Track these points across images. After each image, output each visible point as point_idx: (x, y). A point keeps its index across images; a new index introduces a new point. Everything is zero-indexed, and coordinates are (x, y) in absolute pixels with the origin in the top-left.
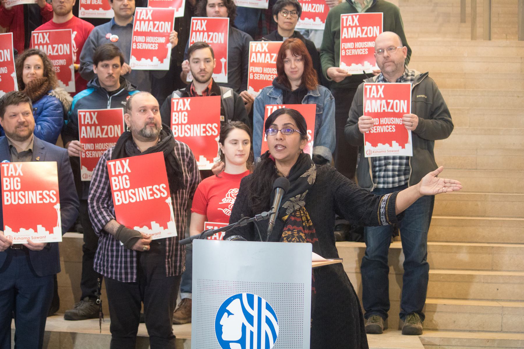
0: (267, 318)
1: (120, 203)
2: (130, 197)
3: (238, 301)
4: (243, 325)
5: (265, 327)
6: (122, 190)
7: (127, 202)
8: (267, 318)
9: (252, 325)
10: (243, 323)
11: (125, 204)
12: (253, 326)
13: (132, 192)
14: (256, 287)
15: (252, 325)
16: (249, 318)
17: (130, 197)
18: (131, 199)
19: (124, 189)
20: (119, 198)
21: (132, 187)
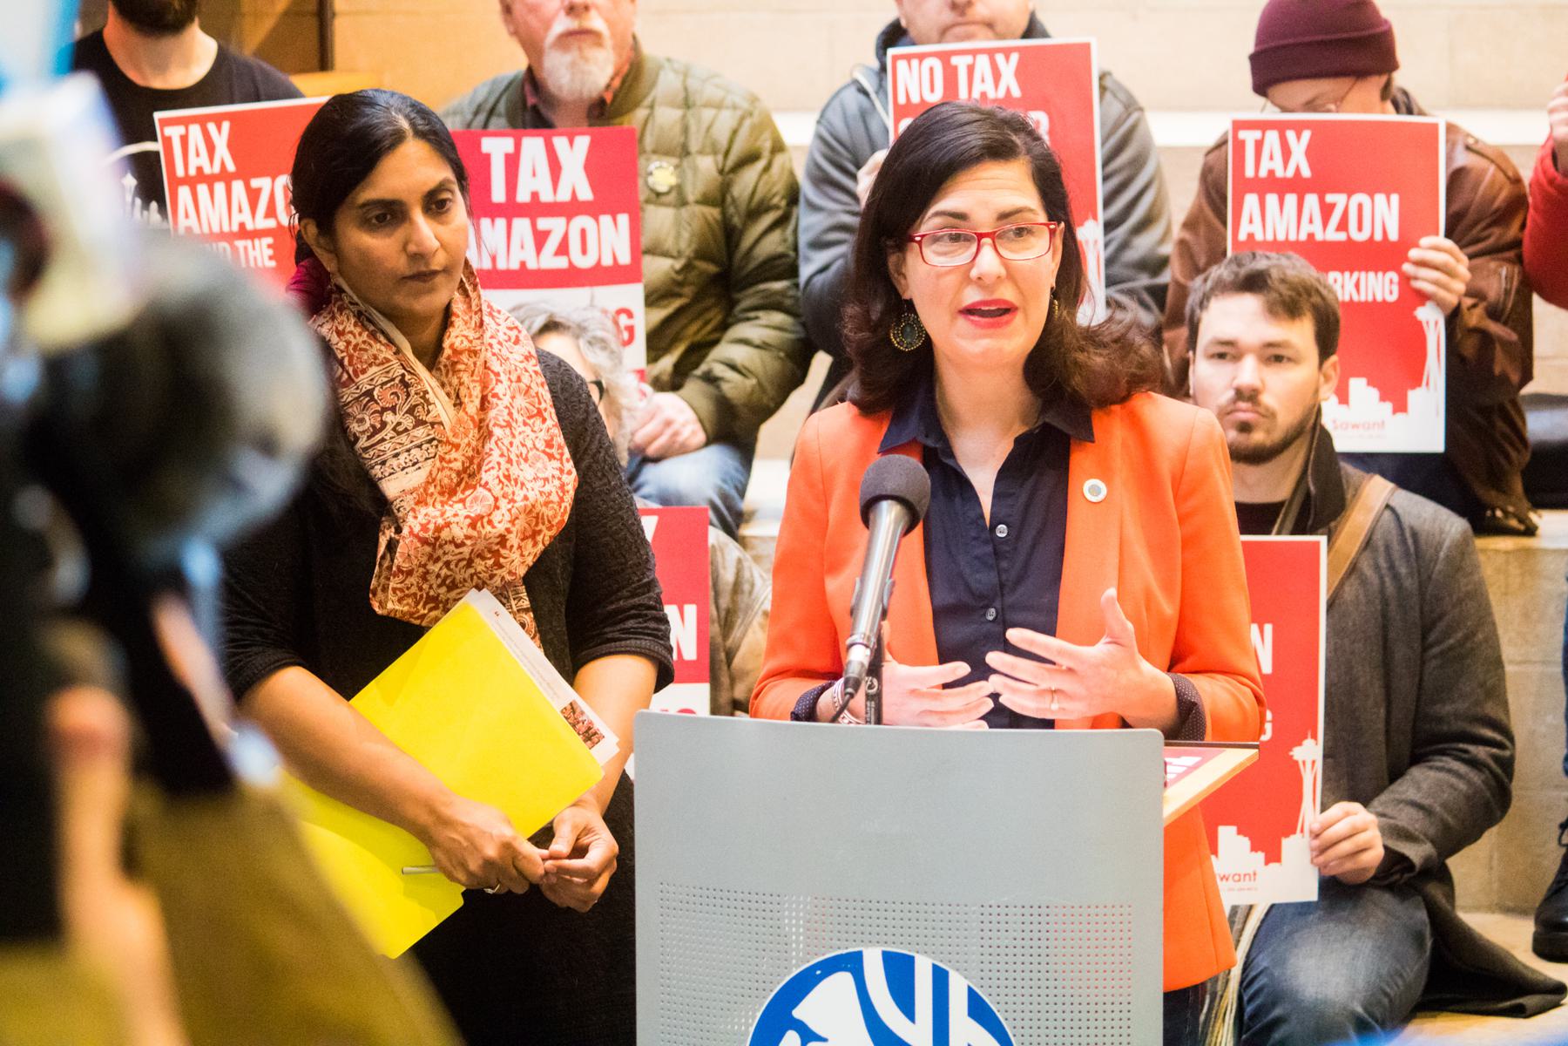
3: (843, 980)
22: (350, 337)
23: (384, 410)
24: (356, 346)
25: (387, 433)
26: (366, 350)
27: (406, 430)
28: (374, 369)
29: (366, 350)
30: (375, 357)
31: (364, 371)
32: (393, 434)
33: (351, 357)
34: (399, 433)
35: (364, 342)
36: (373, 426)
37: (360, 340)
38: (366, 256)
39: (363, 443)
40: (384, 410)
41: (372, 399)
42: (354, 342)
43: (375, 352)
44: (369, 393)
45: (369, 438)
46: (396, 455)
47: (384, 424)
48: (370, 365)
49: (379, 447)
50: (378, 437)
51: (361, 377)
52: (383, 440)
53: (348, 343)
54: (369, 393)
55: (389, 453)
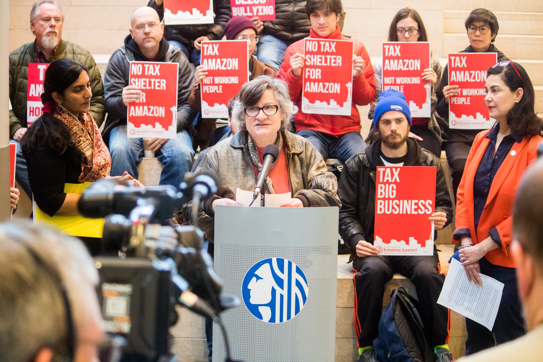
0: (297, 281)
1: (382, 212)
2: (393, 208)
4: (273, 288)
5: (295, 290)
6: (387, 199)
7: (389, 213)
8: (297, 281)
9: (282, 288)
10: (273, 287)
11: (386, 214)
12: (283, 289)
13: (396, 203)
14: (297, 257)
15: (282, 288)
16: (279, 282)
17: (393, 208)
18: (394, 210)
19: (389, 199)
20: (382, 207)
21: (398, 197)
22: (67, 119)
23: (80, 137)
24: (70, 121)
25: (82, 142)
26: (72, 122)
27: (85, 141)
28: (75, 127)
29: (72, 122)
30: (75, 124)
31: (73, 128)
32: (83, 142)
33: (69, 124)
34: (84, 142)
35: (72, 120)
36: (79, 141)
37: (71, 120)
38: (75, 99)
39: (77, 145)
40: (80, 137)
41: (77, 134)
42: (69, 120)
43: (75, 123)
44: (76, 133)
45: (78, 144)
46: (85, 147)
47: (81, 140)
48: (74, 126)
49: (81, 146)
50: (80, 143)
51: (73, 129)
52: (81, 144)
53: (68, 121)
54: (76, 133)
55: (84, 147)
